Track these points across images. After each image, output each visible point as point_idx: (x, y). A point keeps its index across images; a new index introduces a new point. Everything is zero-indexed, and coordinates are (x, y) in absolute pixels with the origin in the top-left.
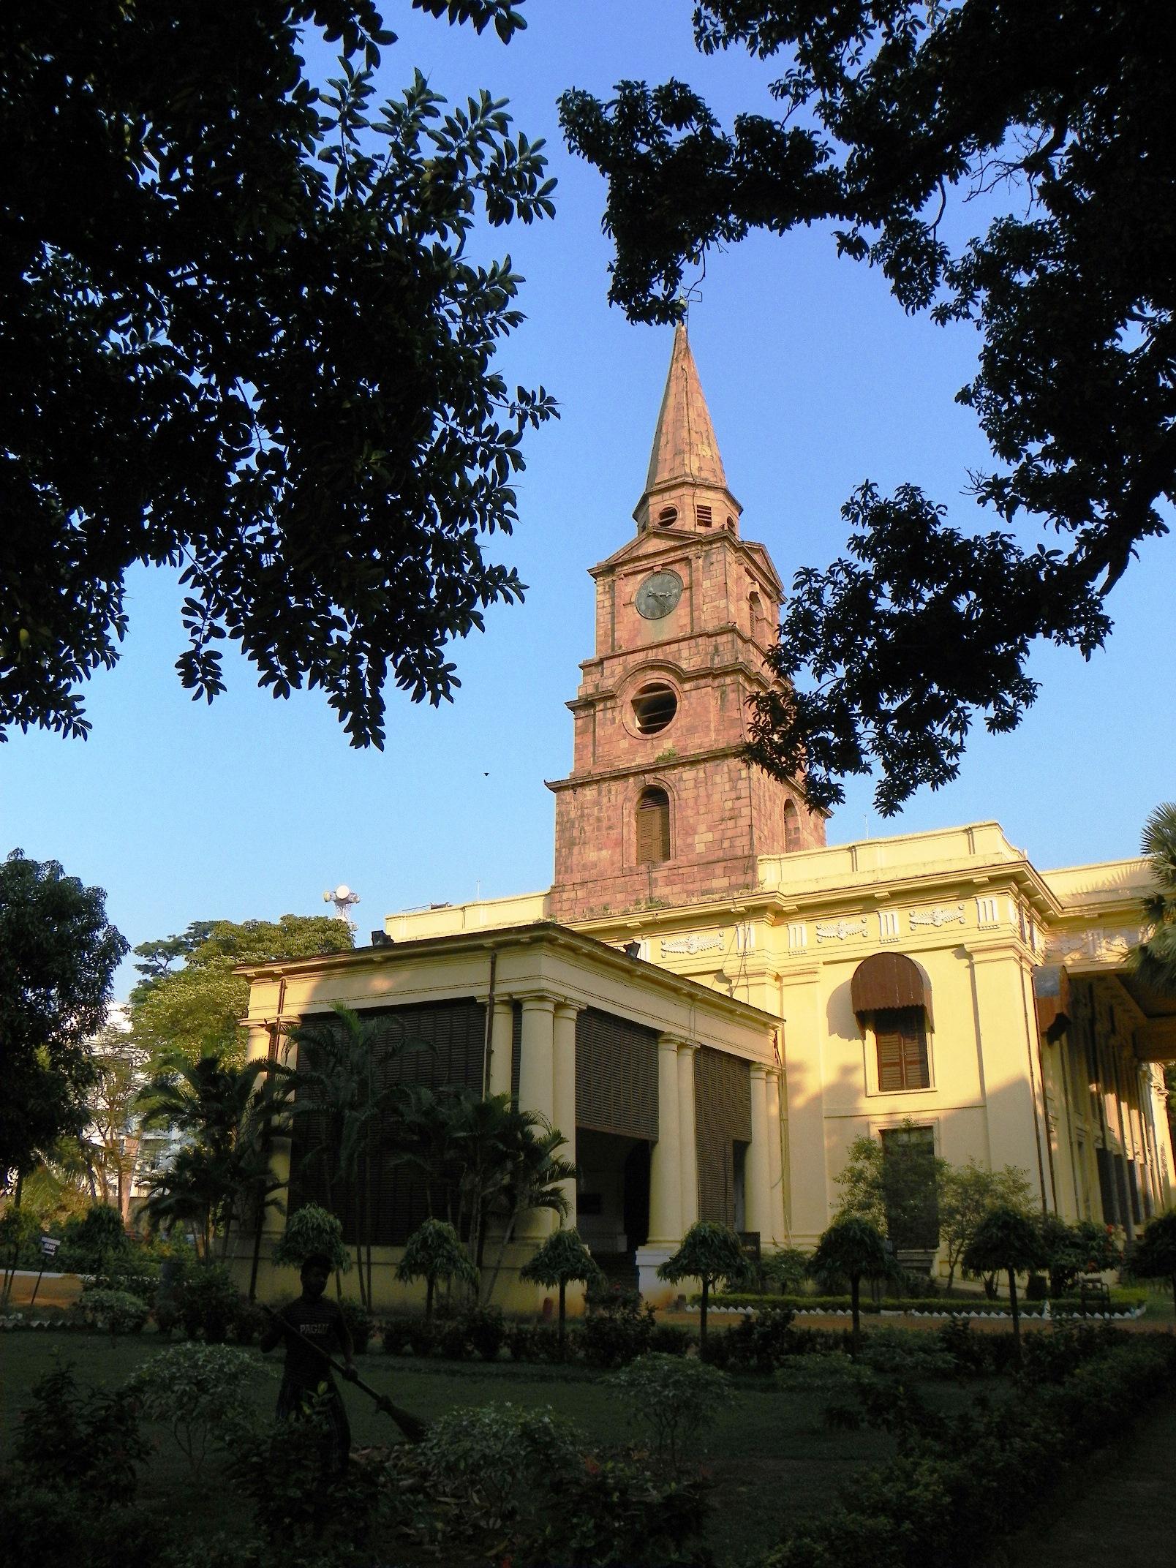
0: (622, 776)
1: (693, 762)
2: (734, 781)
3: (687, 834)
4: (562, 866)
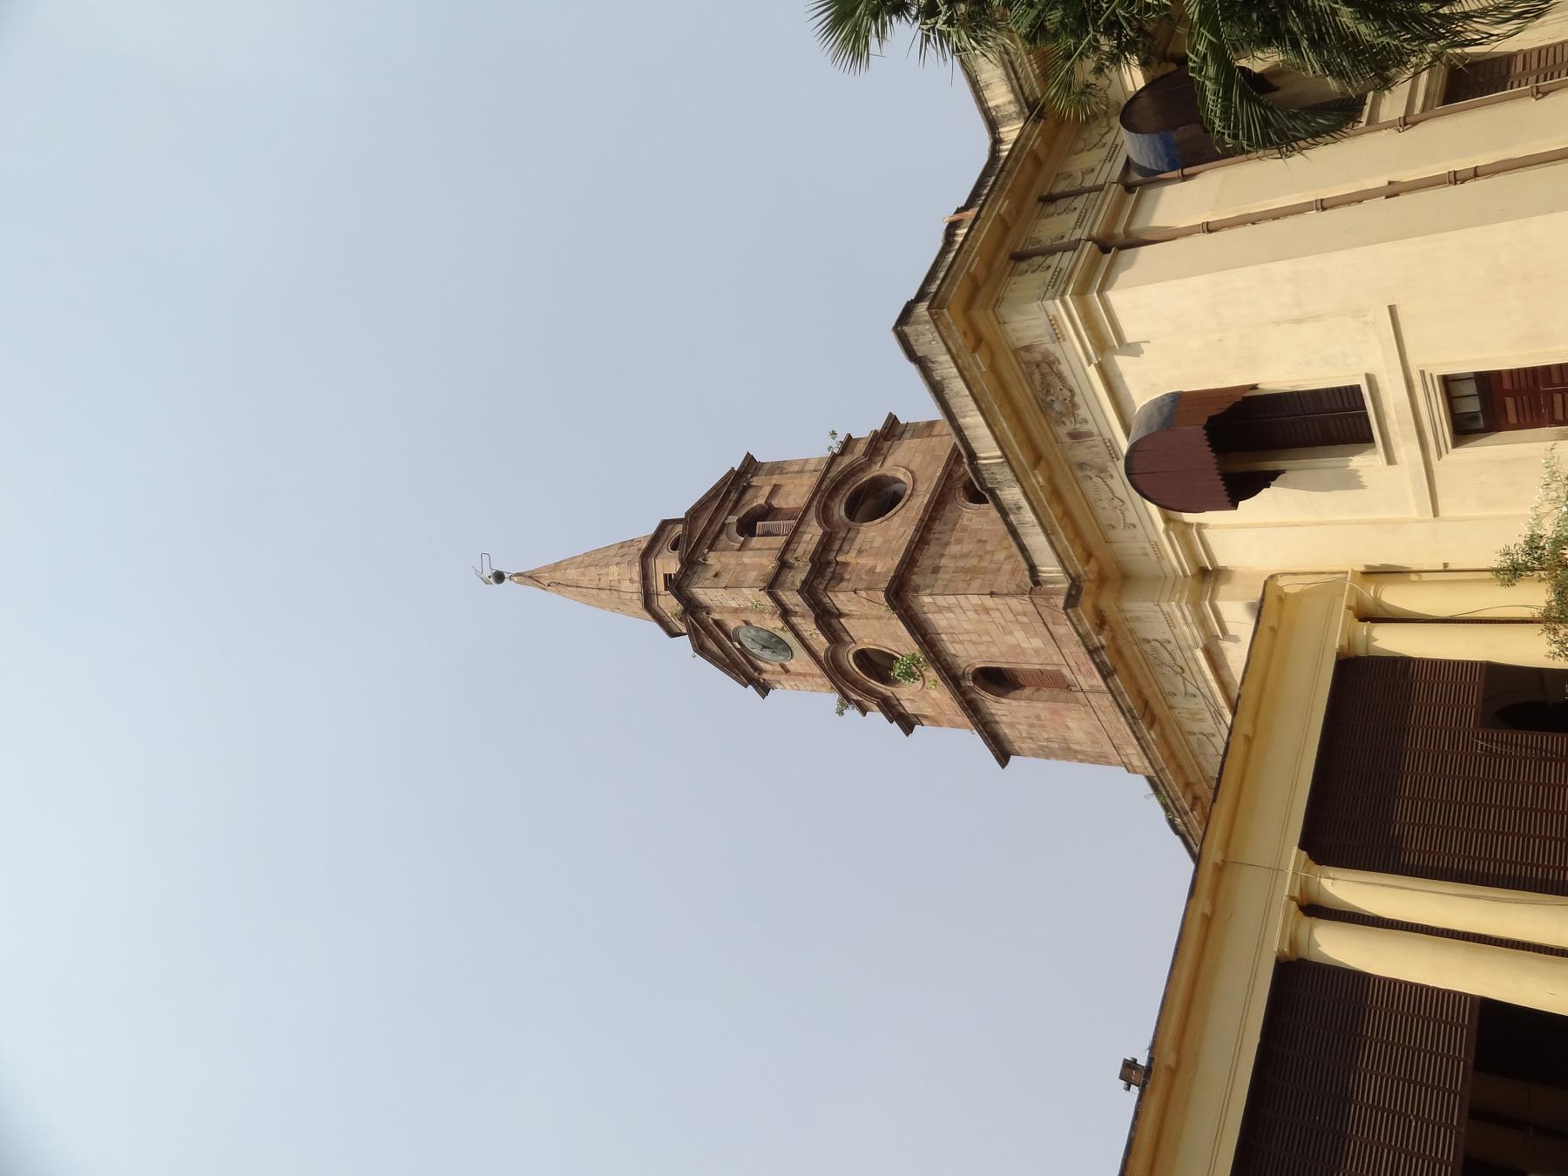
2: (940, 610)
3: (1023, 652)
4: (1101, 759)
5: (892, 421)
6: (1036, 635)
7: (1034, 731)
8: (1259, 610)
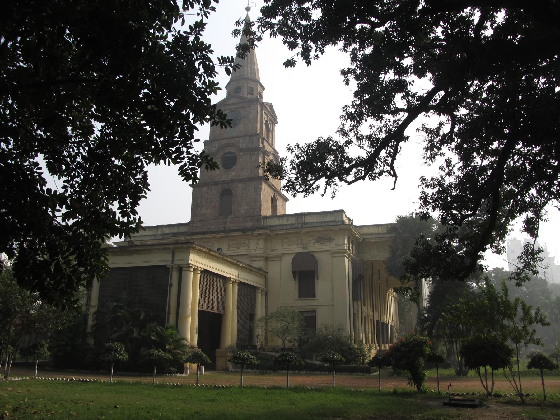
1: (242, 181)
8: (260, 269)
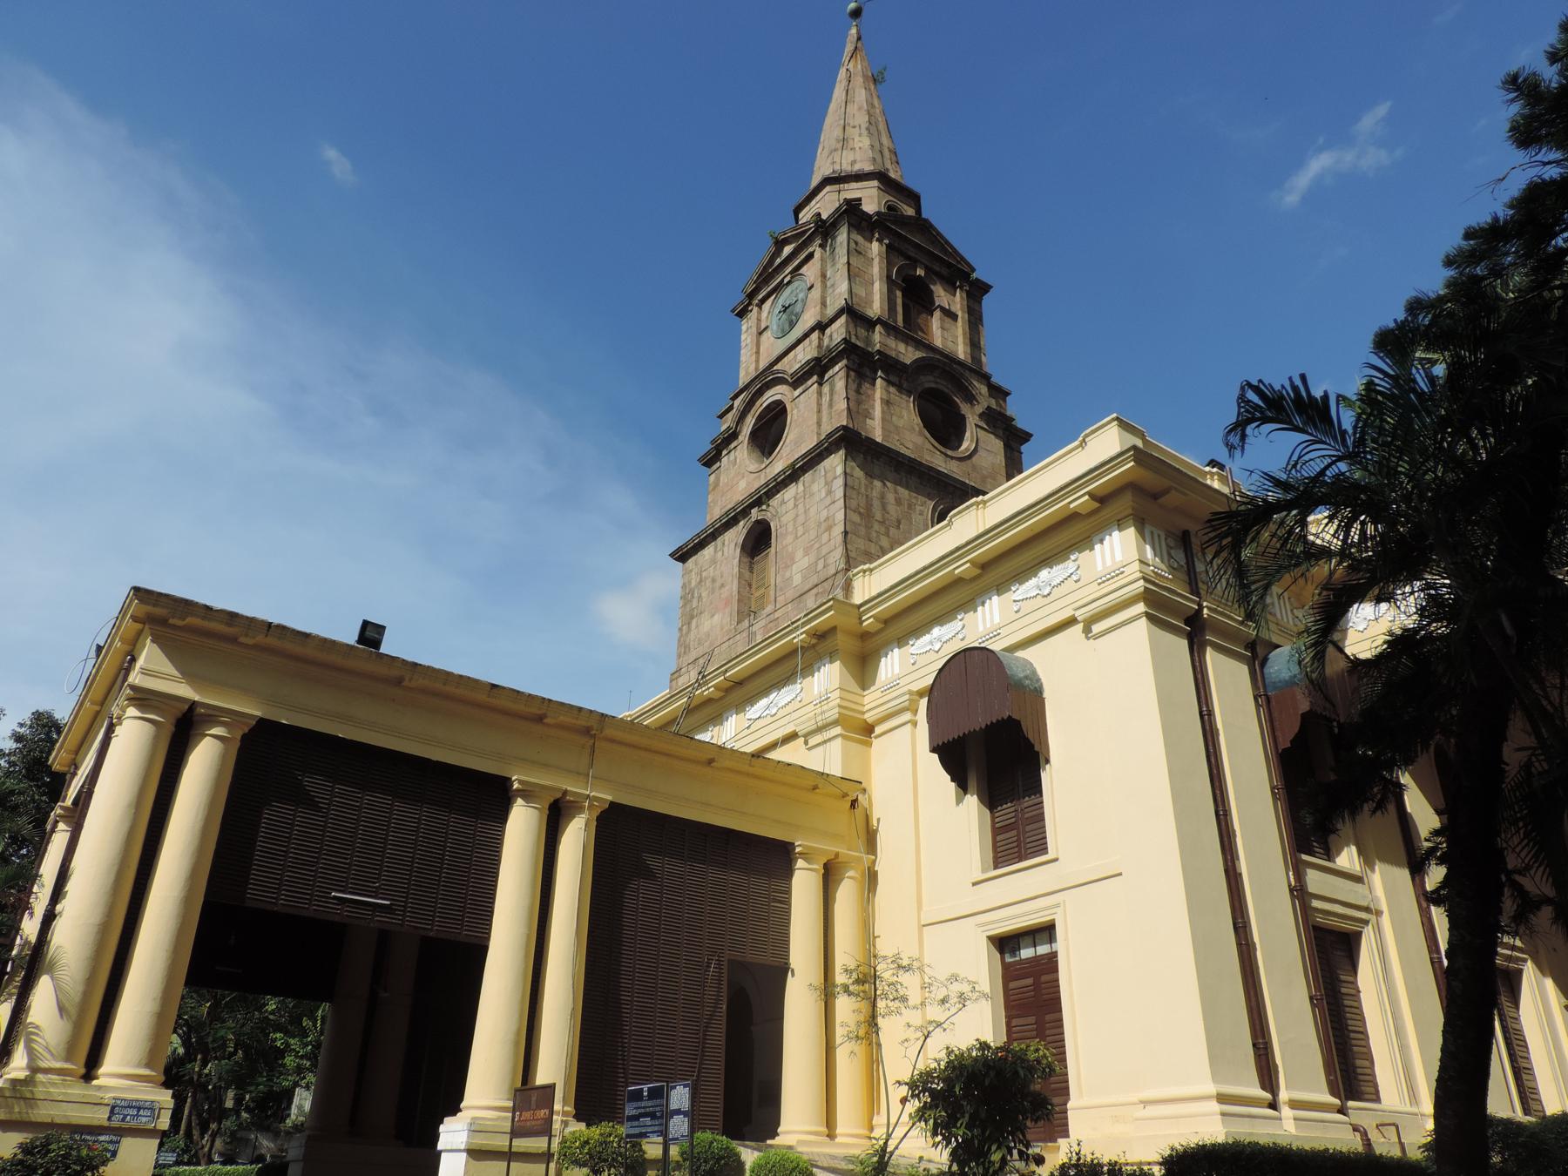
0: (730, 522)
3: (787, 567)
4: (684, 647)
5: (1025, 437)
6: (805, 578)
7: (708, 583)
